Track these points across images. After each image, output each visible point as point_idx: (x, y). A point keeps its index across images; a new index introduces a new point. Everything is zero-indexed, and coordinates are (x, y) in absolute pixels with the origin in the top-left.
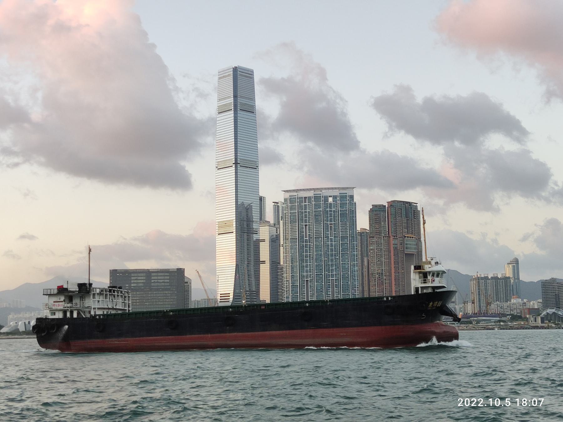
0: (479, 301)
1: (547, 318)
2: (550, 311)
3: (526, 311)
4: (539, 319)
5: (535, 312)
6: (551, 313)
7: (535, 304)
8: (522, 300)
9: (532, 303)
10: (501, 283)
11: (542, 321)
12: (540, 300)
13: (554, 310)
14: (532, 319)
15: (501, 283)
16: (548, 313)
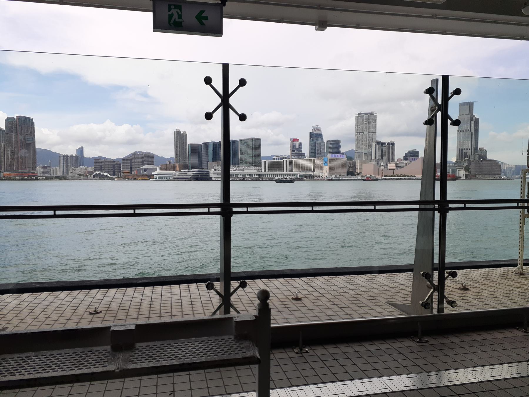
0: (64, 167)
1: (96, 175)
2: (98, 172)
3: (87, 172)
4: (92, 176)
5: (91, 173)
6: (98, 173)
7: (91, 169)
8: (85, 167)
9: (89, 168)
10: (75, 159)
11: (94, 177)
12: (93, 167)
13: (99, 172)
14: (89, 176)
15: (75, 159)
16: (96, 173)
